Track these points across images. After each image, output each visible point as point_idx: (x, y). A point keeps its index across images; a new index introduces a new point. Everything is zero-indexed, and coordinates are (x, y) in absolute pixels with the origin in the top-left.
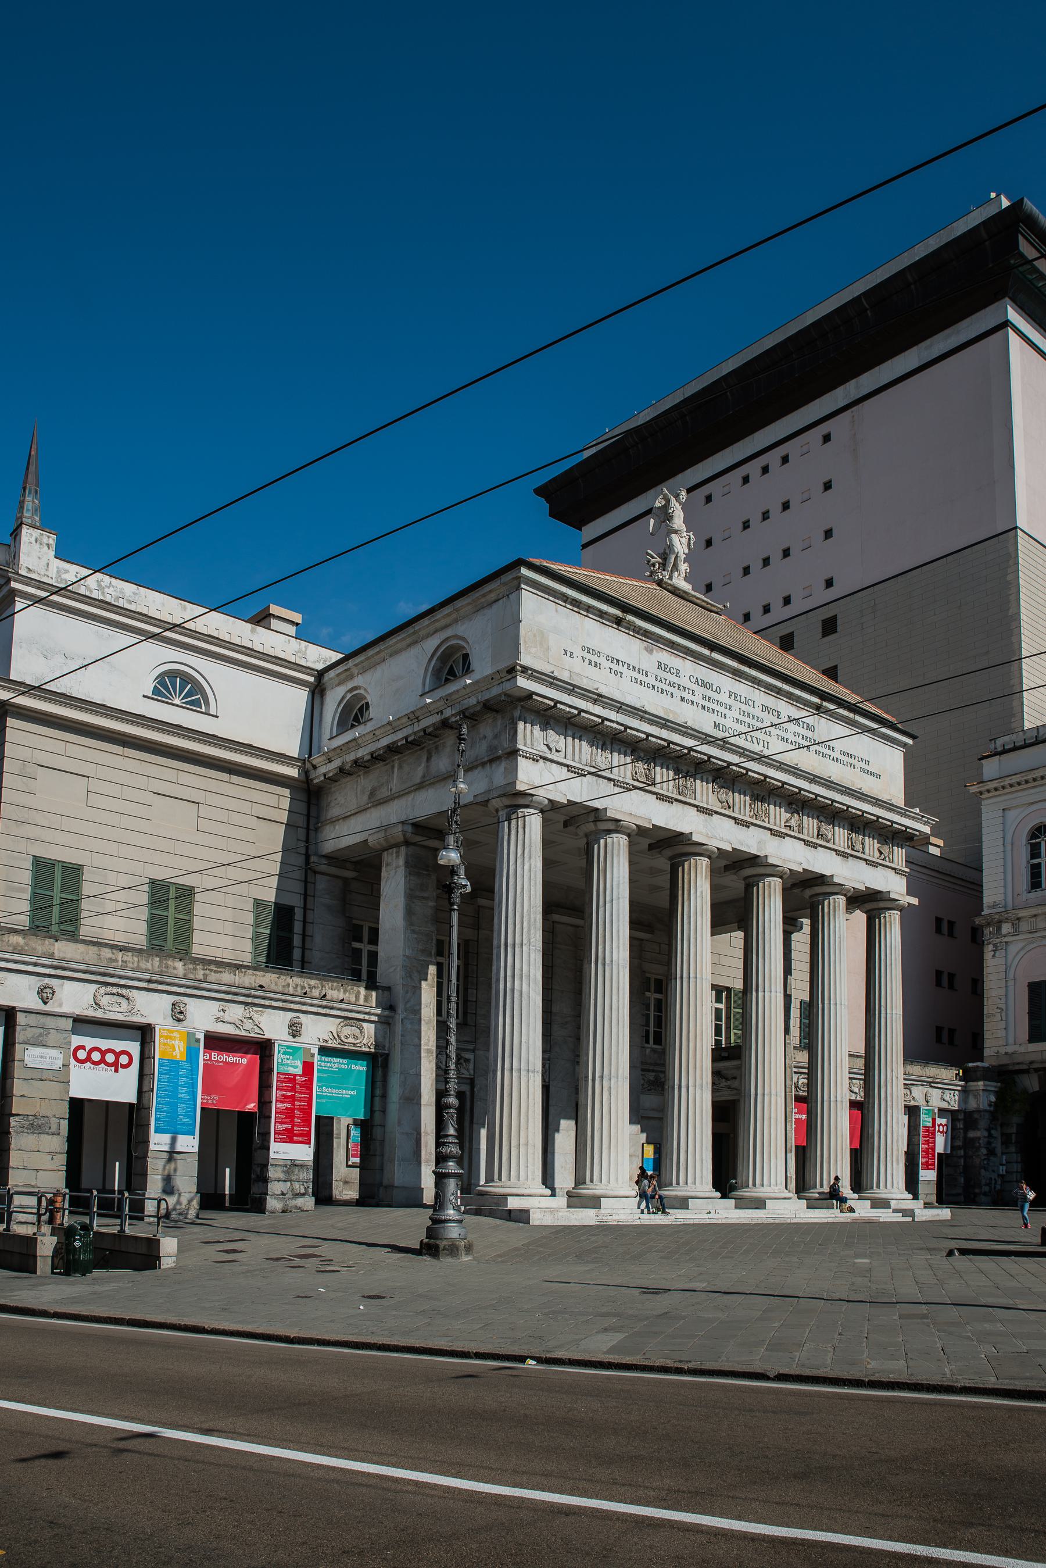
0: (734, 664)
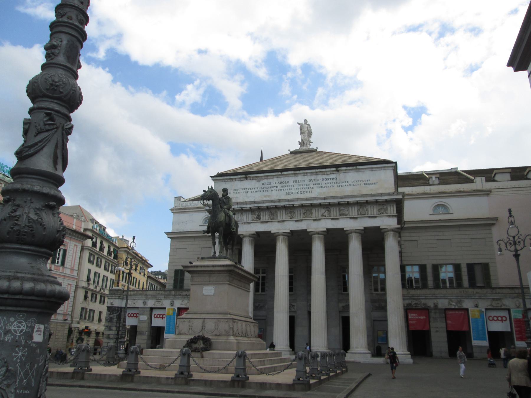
0: (292, 172)
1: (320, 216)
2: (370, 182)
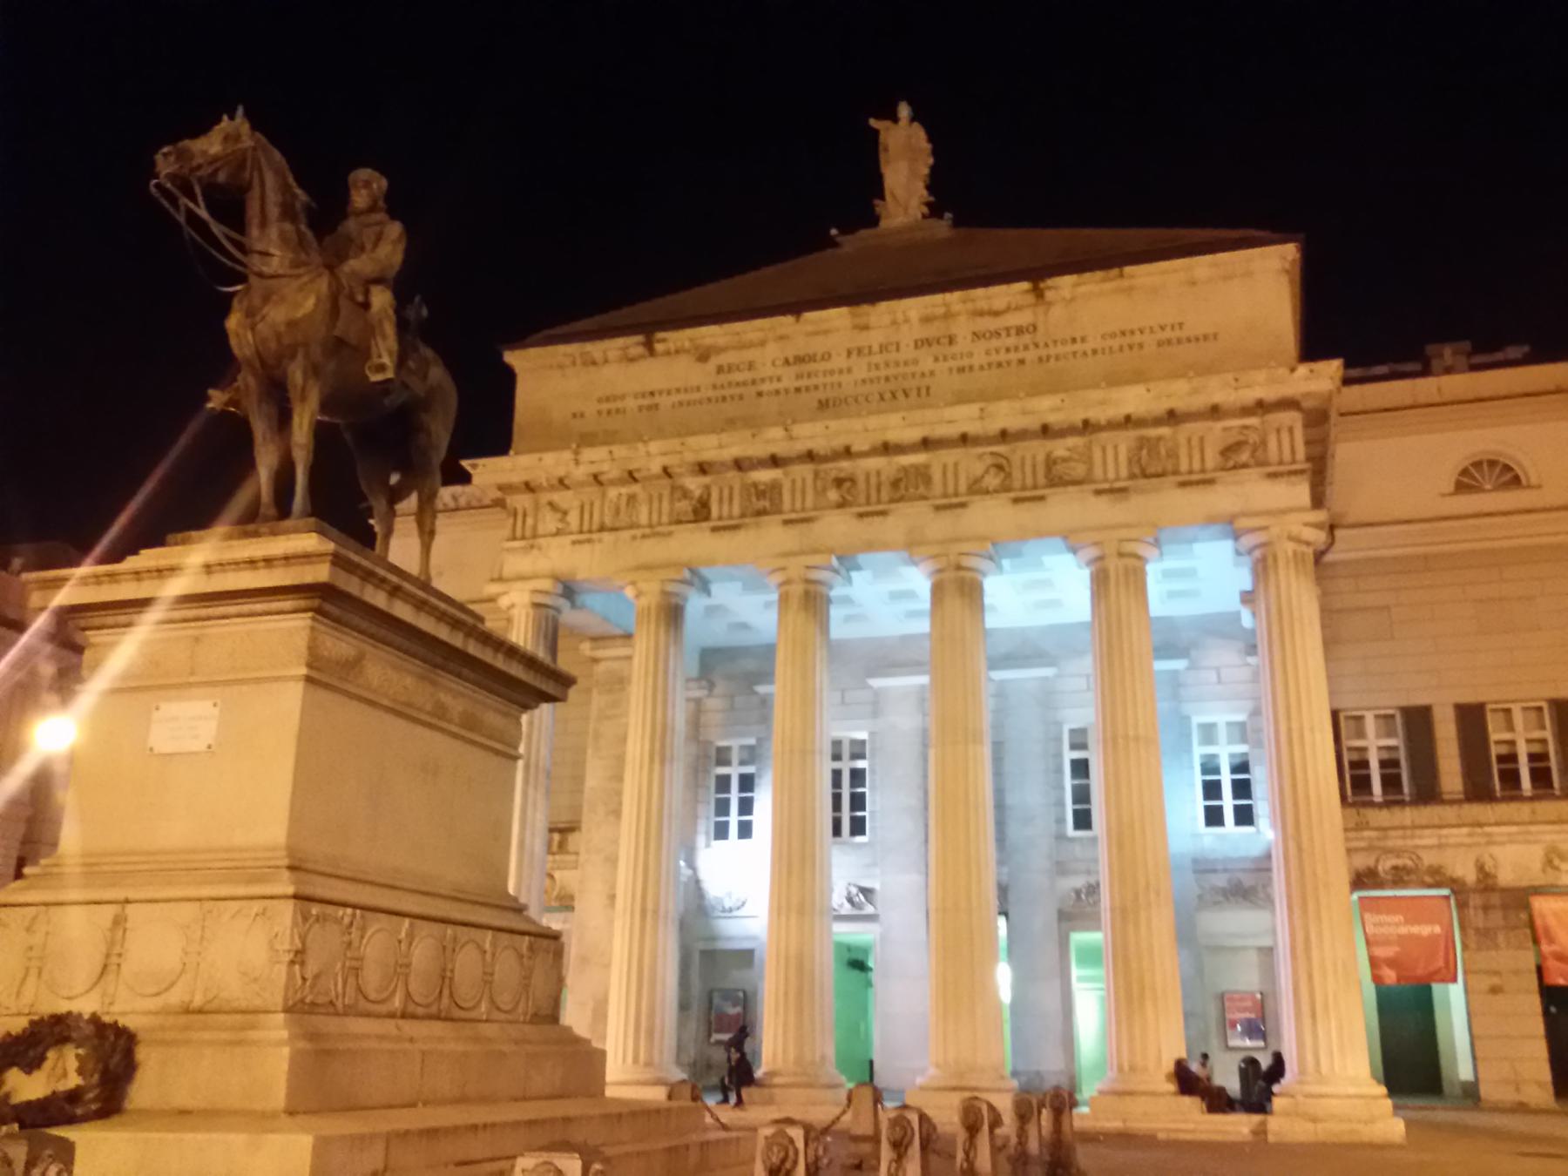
0: (844, 310)
1: (963, 488)
2: (1183, 334)
